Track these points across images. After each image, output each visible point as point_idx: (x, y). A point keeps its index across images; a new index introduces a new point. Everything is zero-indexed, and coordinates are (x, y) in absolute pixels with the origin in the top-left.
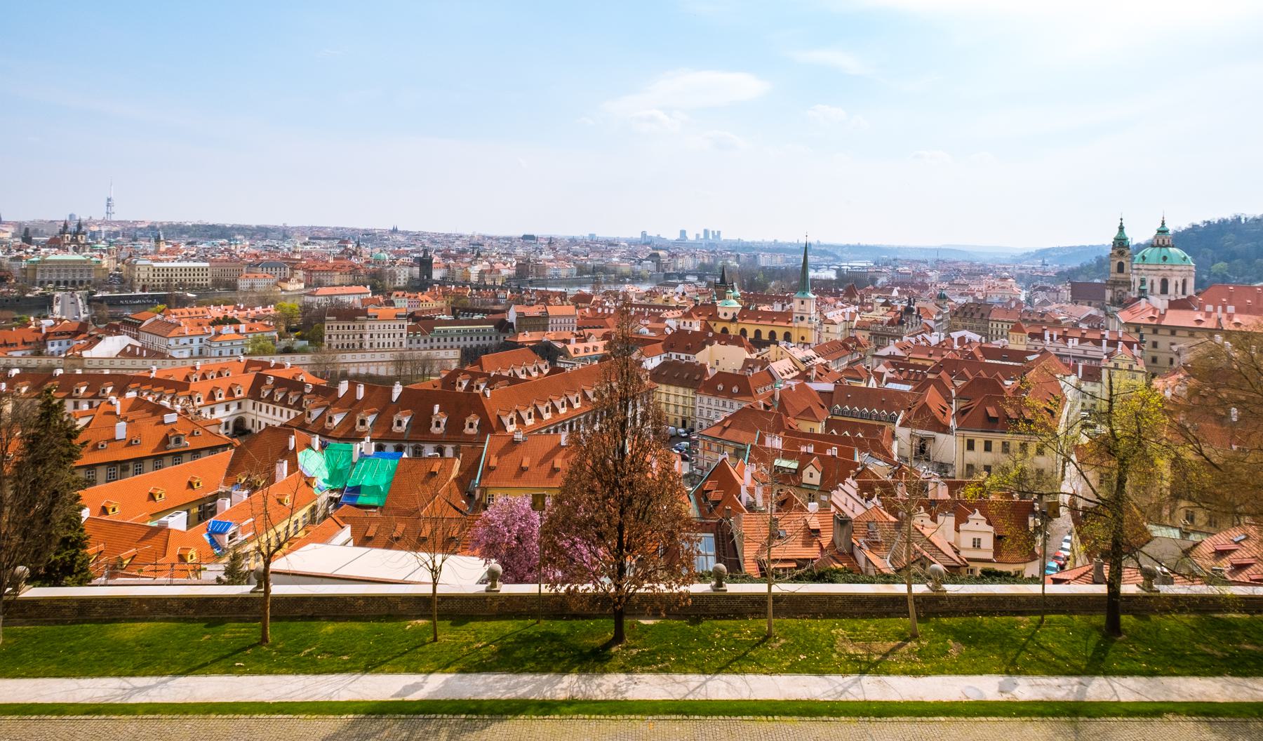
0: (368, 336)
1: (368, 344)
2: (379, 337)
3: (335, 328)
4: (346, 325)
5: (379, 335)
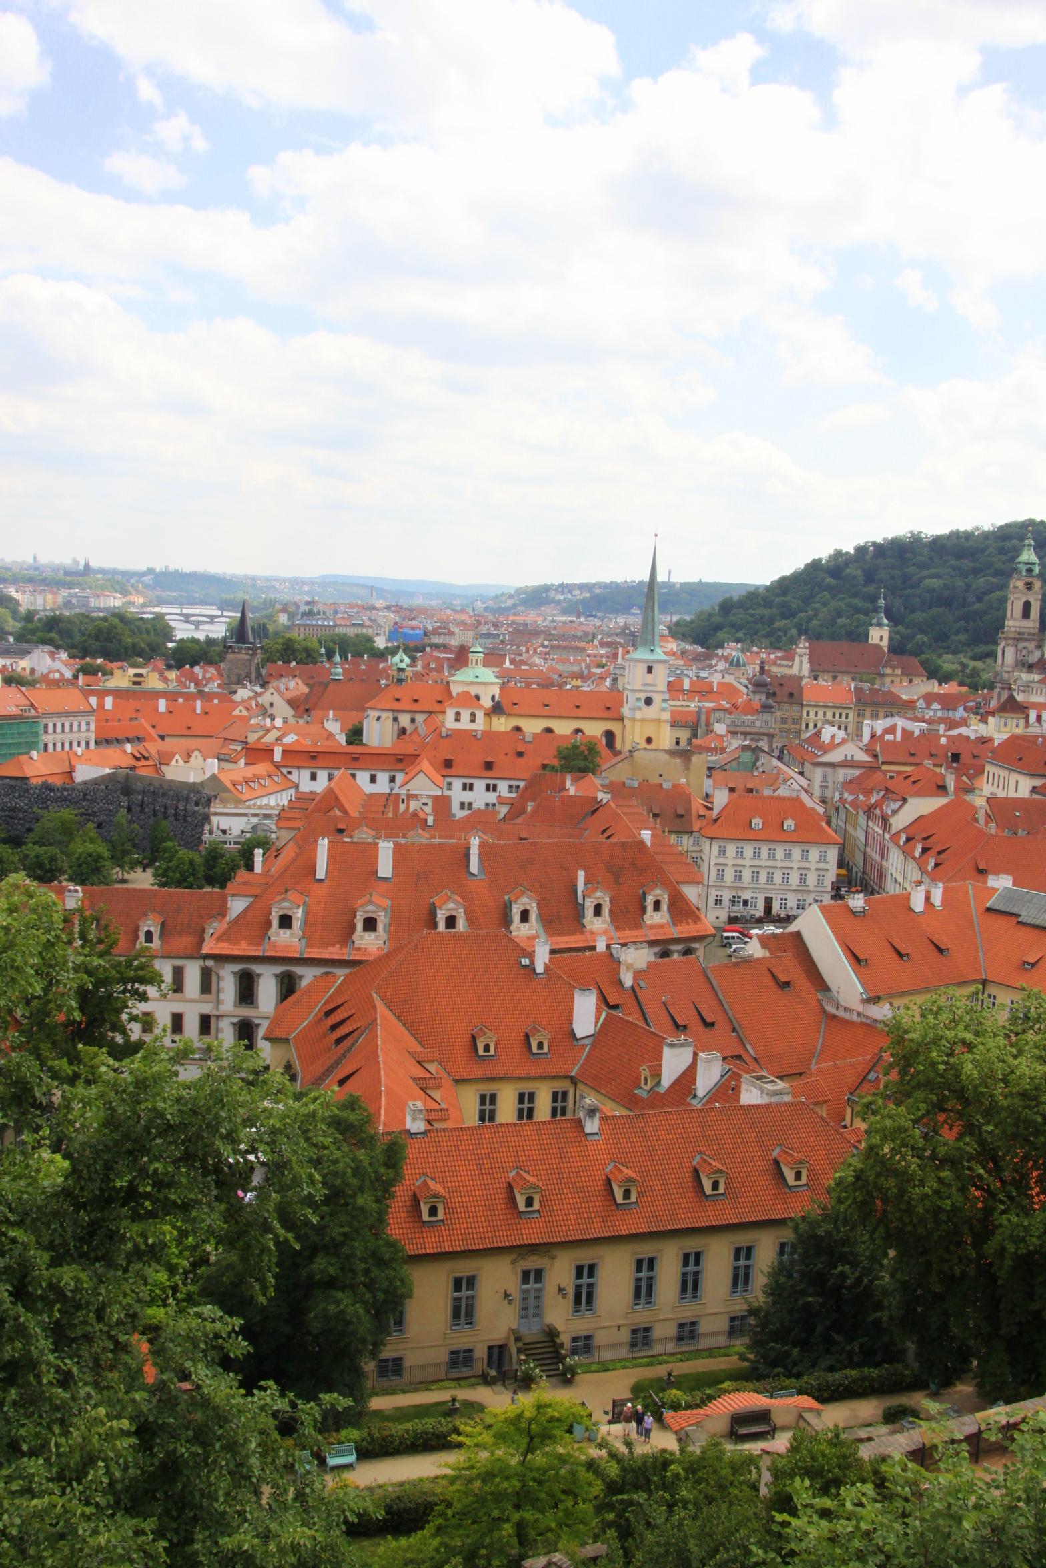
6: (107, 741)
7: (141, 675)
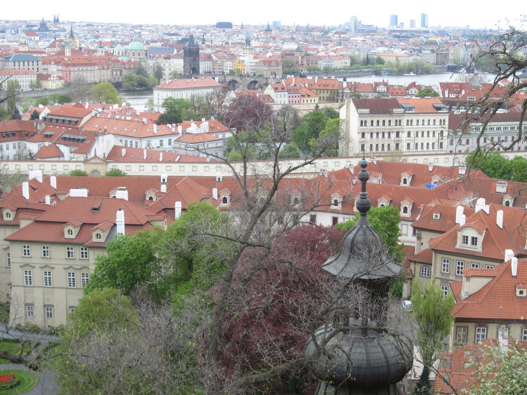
0: (406, 134)
1: (405, 145)
3: (369, 123)
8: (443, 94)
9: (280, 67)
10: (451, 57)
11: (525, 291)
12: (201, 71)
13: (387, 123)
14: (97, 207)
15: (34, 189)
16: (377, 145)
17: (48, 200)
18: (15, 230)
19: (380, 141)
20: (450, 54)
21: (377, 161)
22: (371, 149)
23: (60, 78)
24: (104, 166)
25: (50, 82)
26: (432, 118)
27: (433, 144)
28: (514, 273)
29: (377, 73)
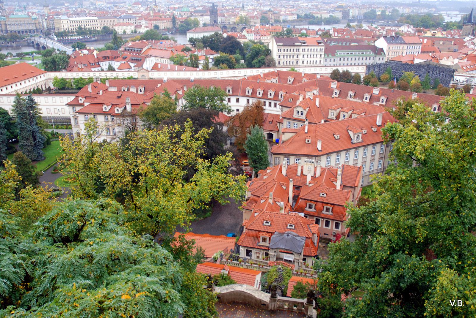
0: (302, 56)
2: (308, 57)
3: (282, 51)
4: (289, 49)
5: (308, 55)
6: (424, 52)
7: (435, 33)
8: (334, 35)
9: (259, 20)
10: (351, 14)
11: (310, 140)
12: (218, 23)
13: (292, 50)
14: (119, 96)
15: (95, 87)
16: (287, 62)
17: (101, 92)
18: (82, 107)
19: (288, 60)
20: (350, 13)
21: (278, 71)
22: (284, 64)
23: (147, 27)
24: (147, 73)
25: (141, 29)
26: (316, 48)
27: (316, 61)
28: (306, 131)
29: (310, 24)
